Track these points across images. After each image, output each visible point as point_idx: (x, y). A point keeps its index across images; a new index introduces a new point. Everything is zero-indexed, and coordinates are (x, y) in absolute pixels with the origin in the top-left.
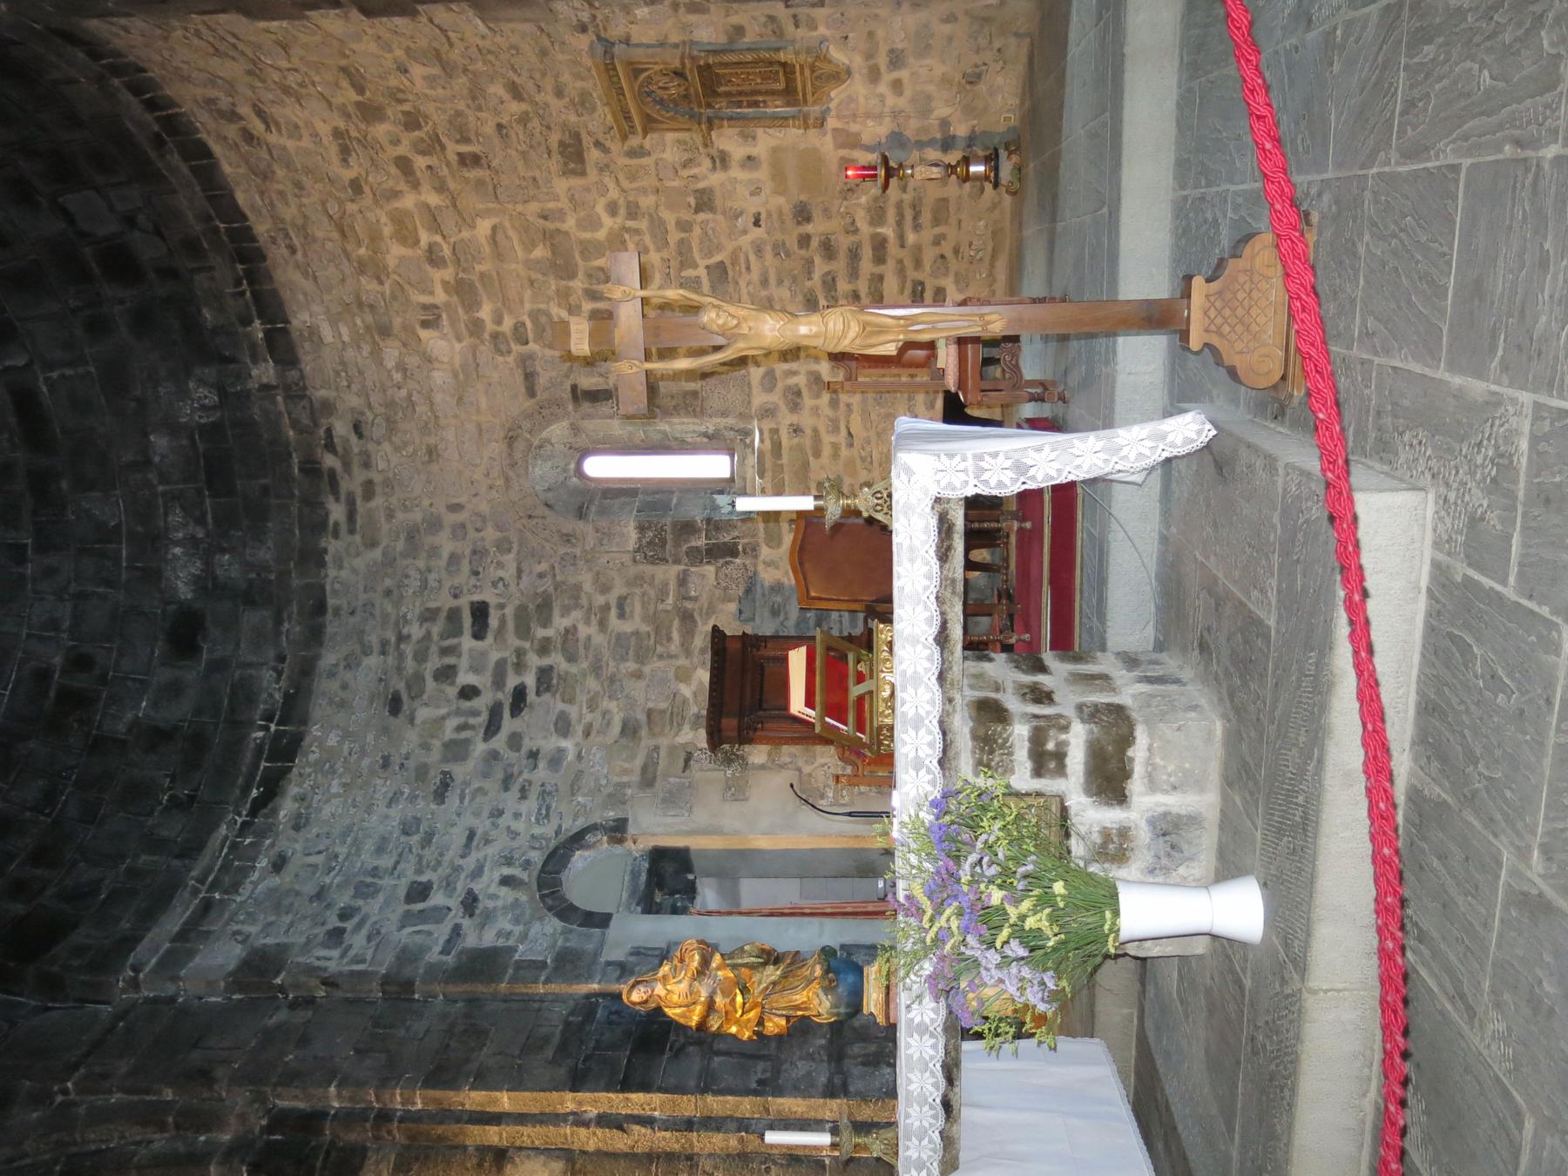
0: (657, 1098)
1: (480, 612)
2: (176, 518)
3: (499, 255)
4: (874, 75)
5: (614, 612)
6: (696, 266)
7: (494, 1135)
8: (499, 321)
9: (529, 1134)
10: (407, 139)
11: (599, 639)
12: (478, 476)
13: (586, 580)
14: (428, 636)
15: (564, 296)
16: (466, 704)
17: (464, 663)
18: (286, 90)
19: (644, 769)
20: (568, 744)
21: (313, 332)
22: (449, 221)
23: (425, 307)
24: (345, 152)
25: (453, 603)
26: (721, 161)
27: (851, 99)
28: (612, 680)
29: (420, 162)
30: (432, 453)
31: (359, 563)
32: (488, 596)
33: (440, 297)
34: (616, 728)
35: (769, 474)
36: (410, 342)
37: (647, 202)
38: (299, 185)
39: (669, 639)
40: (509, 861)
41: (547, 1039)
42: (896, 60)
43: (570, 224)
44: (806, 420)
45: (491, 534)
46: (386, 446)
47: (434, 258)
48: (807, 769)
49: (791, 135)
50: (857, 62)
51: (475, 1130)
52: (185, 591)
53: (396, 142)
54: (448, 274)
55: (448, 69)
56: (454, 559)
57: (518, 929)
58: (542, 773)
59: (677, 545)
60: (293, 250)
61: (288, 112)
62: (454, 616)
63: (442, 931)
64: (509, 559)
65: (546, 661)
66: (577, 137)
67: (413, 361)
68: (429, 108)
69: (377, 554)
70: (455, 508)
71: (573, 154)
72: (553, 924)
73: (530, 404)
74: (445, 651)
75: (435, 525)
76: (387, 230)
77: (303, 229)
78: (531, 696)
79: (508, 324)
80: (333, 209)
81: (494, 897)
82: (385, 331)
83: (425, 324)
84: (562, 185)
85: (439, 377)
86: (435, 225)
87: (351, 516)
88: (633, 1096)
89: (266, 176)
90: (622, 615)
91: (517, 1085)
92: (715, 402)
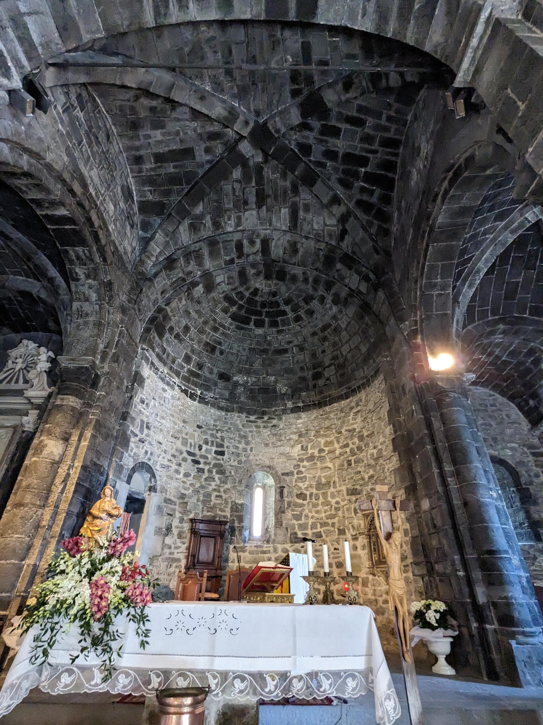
0: (70, 495)
1: (222, 453)
2: (253, 379)
3: (322, 469)
5: (218, 494)
6: (321, 528)
7: (74, 439)
8: (303, 467)
9: (71, 450)
10: (354, 447)
12: (260, 457)
13: (228, 486)
14: (218, 438)
15: (311, 486)
16: (197, 447)
17: (209, 447)
18: (365, 418)
19: (170, 500)
20: (181, 476)
21: (300, 418)
23: (307, 447)
24: (349, 431)
25: (225, 446)
26: (355, 538)
27: (380, 585)
28: (198, 492)
29: (348, 450)
30: (267, 445)
31: (238, 422)
32: (226, 457)
33: (310, 451)
34: (184, 492)
35: (256, 549)
36: (297, 442)
37: (340, 513)
38: (340, 419)
39: (208, 511)
40: (151, 454)
41: (99, 459)
43: (332, 490)
45: (244, 459)
46: (269, 433)
47: (321, 451)
48: (160, 559)
51: (78, 433)
52: (235, 379)
53: (353, 444)
54: (316, 454)
55: (377, 459)
56: (237, 448)
57: (132, 454)
58: (174, 467)
59: (236, 516)
60: (322, 415)
61: (359, 419)
62: (222, 446)
63: (137, 431)
64: (236, 463)
65: (206, 471)
66: (359, 494)
67: (292, 442)
68: (364, 454)
69: (241, 427)
70: (251, 450)
71: (353, 492)
72: (131, 465)
73: (280, 473)
74: (212, 442)
75: (247, 443)
76: (328, 439)
77: (327, 418)
78: (197, 466)
79: (303, 470)
80: (333, 427)
81: (143, 448)
82: (300, 436)
83: (302, 446)
84: (344, 488)
85: (288, 449)
86: (330, 452)
88: (74, 487)
89: (342, 411)
90: (217, 496)
91: (89, 448)
92: (279, 532)
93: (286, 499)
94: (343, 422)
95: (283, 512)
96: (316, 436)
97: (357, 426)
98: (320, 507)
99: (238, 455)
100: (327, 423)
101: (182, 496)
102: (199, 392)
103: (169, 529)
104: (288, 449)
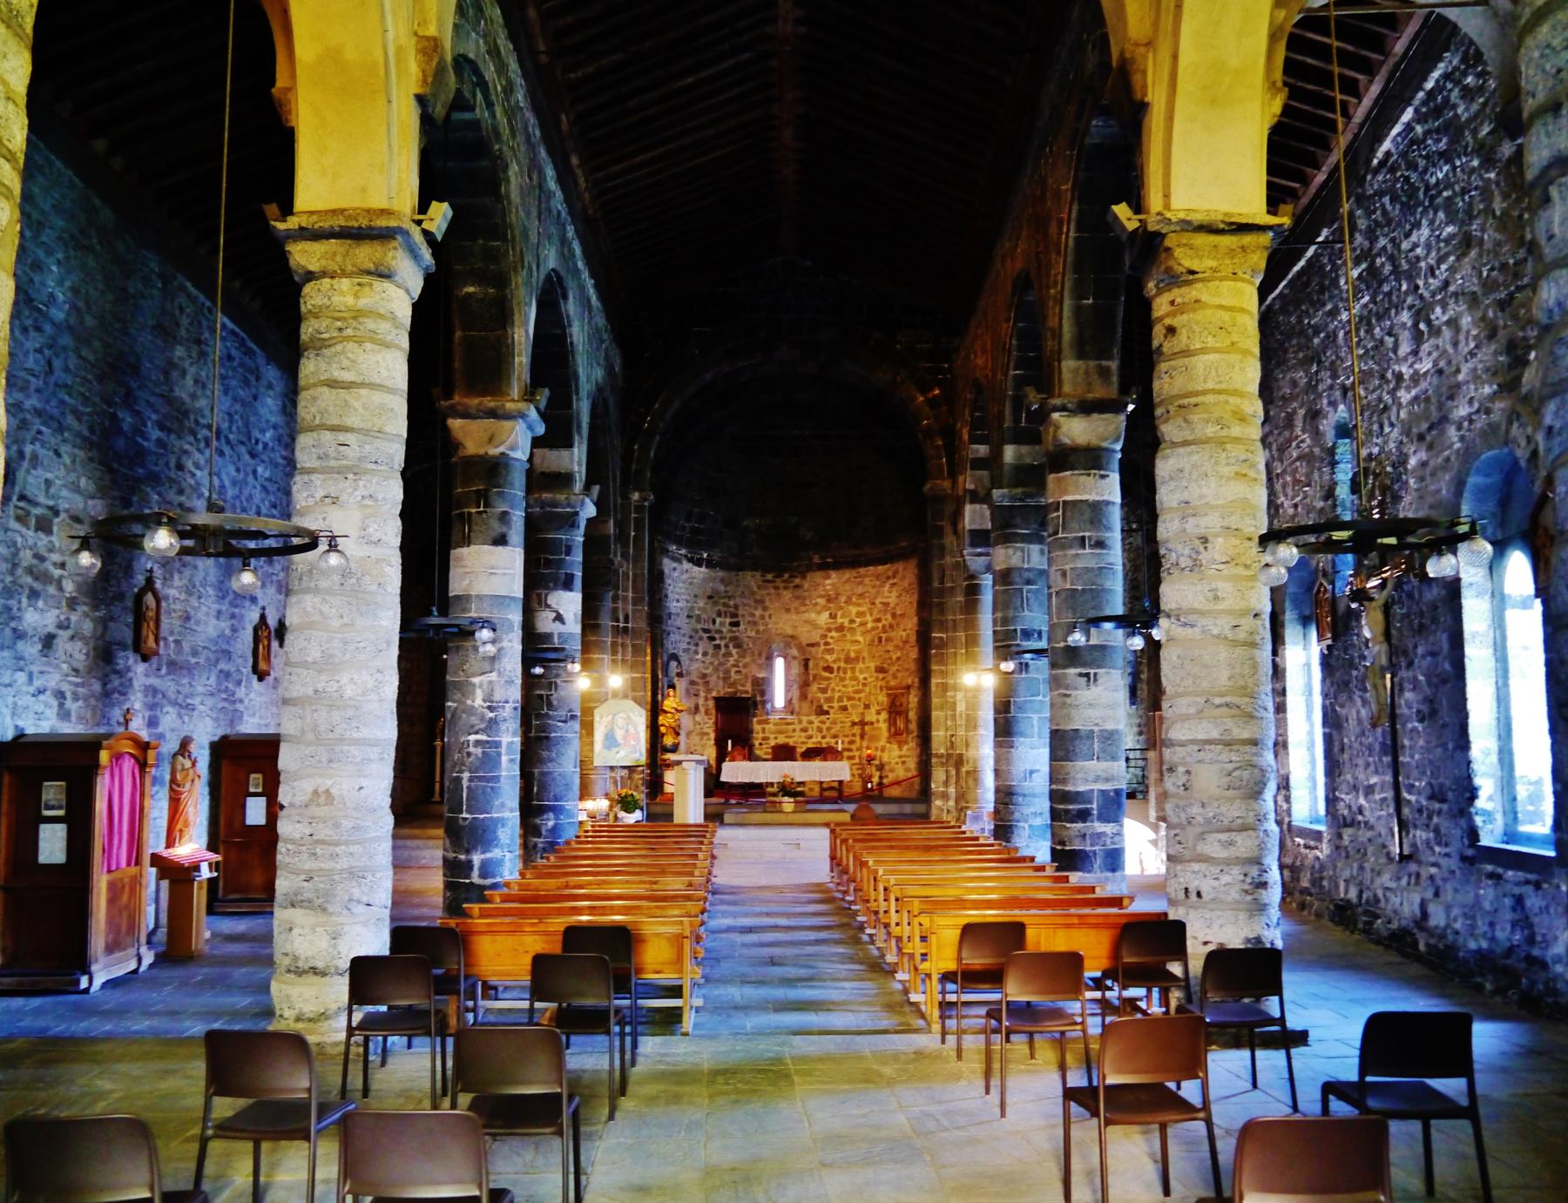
4: (900, 757)
11: (729, 664)
12: (781, 625)
13: (747, 660)
15: (838, 659)
20: (699, 656)
21: (828, 577)
22: (862, 629)
24: (883, 604)
26: (878, 713)
29: (880, 625)
30: (788, 610)
31: (753, 583)
32: (742, 627)
33: (839, 620)
36: (825, 608)
37: (867, 689)
42: (904, 763)
43: (861, 665)
44: (797, 734)
45: (761, 628)
47: (852, 621)
49: (885, 734)
50: (903, 753)
52: (745, 523)
56: (753, 615)
62: (734, 615)
67: (818, 608)
70: (770, 617)
71: (880, 670)
75: (765, 609)
76: (861, 609)
77: (860, 583)
79: (829, 640)
82: (829, 601)
84: (872, 665)
85: (813, 616)
87: (769, 581)
93: (811, 672)
94: (878, 593)
95: (808, 685)
96: (849, 601)
97: (892, 600)
98: (847, 682)
99: (755, 623)
100: (860, 590)
101: (704, 676)
102: (705, 555)
103: (697, 708)
104: (813, 616)
